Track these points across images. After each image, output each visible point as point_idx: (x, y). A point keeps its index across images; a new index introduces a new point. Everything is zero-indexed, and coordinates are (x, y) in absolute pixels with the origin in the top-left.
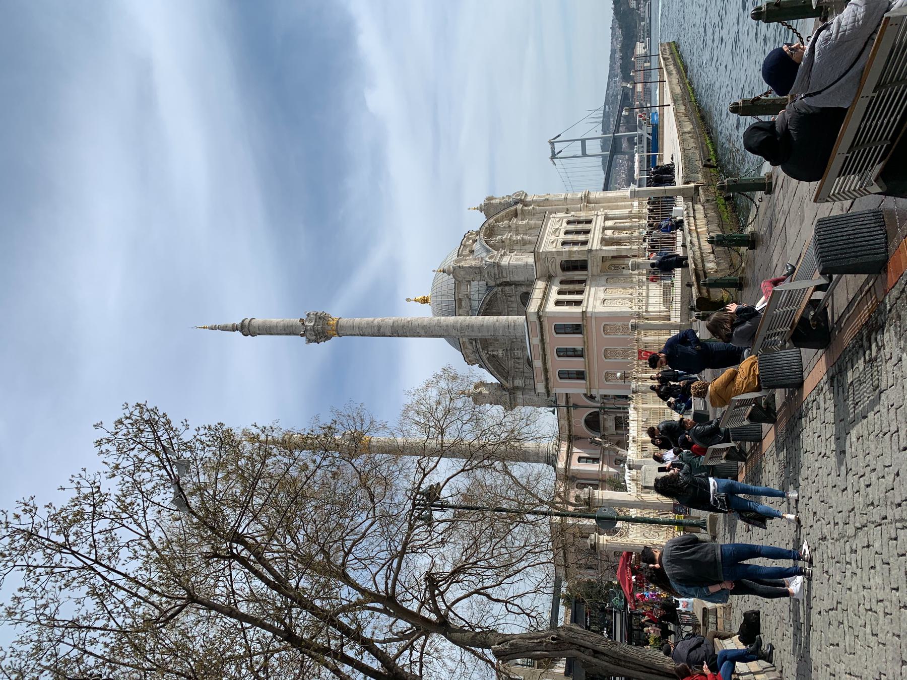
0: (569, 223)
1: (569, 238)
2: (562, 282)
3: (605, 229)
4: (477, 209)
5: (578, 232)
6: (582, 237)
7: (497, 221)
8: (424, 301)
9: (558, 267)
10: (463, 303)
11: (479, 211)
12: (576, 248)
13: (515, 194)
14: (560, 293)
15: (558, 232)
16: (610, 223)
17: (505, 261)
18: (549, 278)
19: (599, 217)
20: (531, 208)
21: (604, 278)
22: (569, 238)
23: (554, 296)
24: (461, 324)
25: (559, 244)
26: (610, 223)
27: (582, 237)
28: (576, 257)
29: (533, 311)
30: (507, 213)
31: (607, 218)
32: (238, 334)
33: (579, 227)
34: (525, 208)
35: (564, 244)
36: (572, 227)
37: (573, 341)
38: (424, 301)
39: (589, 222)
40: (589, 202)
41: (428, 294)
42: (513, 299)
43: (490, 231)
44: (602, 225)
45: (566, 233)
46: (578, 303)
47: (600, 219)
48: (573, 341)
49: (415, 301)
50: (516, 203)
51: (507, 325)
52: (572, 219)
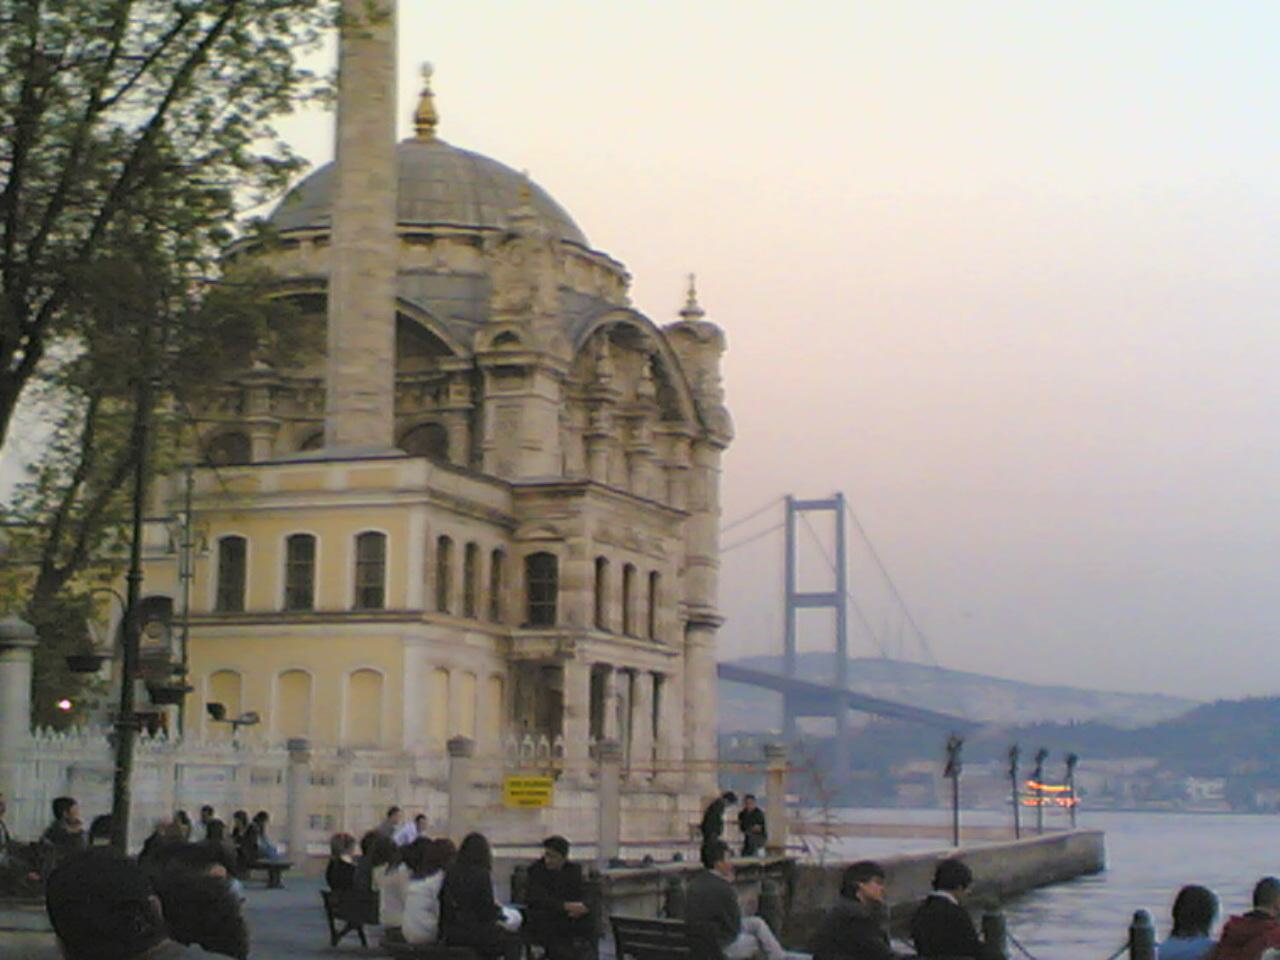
0: (653, 576)
2: (497, 555)
3: (630, 673)
4: (691, 302)
6: (613, 613)
7: (655, 361)
11: (682, 305)
12: (588, 596)
13: (722, 416)
14: (471, 549)
16: (645, 685)
18: (508, 525)
19: (664, 659)
21: (502, 670)
22: (613, 576)
23: (462, 533)
25: (603, 550)
26: (645, 685)
28: (562, 598)
31: (658, 679)
33: (640, 606)
34: (682, 447)
35: (600, 563)
36: (640, 583)
37: (335, 582)
38: (425, 121)
41: (441, 132)
43: (627, 333)
45: (628, 569)
47: (659, 663)
48: (335, 582)
49: (426, 94)
50: (700, 419)
52: (663, 583)
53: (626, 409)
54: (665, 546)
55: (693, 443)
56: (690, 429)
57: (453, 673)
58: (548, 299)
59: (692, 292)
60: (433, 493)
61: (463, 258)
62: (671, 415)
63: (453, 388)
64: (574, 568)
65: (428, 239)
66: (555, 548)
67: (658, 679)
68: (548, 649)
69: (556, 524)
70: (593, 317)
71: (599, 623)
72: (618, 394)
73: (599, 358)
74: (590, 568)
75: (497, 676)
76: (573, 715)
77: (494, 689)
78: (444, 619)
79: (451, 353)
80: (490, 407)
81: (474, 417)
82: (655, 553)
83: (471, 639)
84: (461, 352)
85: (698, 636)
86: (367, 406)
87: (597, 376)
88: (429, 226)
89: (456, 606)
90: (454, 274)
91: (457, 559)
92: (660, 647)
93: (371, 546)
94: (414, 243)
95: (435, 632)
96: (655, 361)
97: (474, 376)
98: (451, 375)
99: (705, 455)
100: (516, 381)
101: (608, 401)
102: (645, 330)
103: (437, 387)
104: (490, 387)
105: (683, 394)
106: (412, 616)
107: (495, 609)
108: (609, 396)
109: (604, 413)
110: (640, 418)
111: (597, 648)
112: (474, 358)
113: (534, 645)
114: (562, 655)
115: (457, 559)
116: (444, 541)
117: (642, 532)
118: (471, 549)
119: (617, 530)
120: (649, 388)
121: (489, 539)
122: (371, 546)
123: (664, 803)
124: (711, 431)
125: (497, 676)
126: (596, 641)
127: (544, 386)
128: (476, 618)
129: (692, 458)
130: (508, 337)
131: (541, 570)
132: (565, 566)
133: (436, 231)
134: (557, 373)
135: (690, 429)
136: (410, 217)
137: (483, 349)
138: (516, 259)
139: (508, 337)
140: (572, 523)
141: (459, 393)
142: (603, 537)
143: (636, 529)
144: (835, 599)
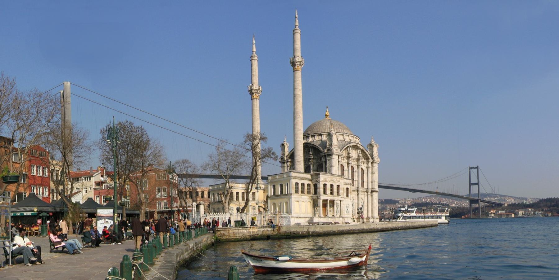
0: (338, 186)
1: (328, 187)
2: (309, 185)
3: (334, 201)
5: (332, 190)
6: (328, 192)
7: (362, 150)
9: (315, 183)
12: (322, 190)
15: (332, 181)
17: (335, 158)
19: (341, 198)
20: (370, 165)
21: (311, 201)
22: (328, 187)
23: (300, 182)
24: (299, 140)
27: (328, 192)
28: (318, 190)
29: (292, 174)
30: (367, 155)
31: (341, 201)
34: (370, 163)
35: (325, 185)
39: (338, 194)
40: (372, 192)
44: (335, 200)
45: (332, 186)
46: (297, 192)
47: (340, 198)
50: (372, 159)
51: (298, 161)
52: (341, 187)
53: (357, 158)
54: (340, 181)
55: (372, 163)
56: (371, 160)
57: (300, 202)
64: (321, 186)
65: (321, 135)
66: (317, 183)
69: (316, 179)
70: (346, 145)
71: (325, 193)
72: (353, 156)
73: (349, 151)
79: (322, 153)
80: (327, 161)
82: (338, 182)
83: (303, 197)
84: (323, 153)
85: (374, 193)
86: (299, 163)
88: (321, 133)
92: (339, 196)
94: (319, 136)
96: (362, 150)
97: (325, 156)
98: (322, 156)
101: (351, 158)
102: (359, 145)
103: (321, 159)
107: (309, 193)
108: (350, 157)
109: (350, 159)
110: (359, 160)
112: (325, 153)
114: (318, 198)
117: (335, 180)
119: (329, 179)
120: (361, 155)
121: (306, 182)
123: (341, 219)
124: (374, 161)
131: (316, 187)
132: (318, 185)
133: (322, 134)
134: (337, 154)
136: (319, 132)
138: (330, 138)
140: (319, 179)
141: (324, 159)
143: (333, 179)
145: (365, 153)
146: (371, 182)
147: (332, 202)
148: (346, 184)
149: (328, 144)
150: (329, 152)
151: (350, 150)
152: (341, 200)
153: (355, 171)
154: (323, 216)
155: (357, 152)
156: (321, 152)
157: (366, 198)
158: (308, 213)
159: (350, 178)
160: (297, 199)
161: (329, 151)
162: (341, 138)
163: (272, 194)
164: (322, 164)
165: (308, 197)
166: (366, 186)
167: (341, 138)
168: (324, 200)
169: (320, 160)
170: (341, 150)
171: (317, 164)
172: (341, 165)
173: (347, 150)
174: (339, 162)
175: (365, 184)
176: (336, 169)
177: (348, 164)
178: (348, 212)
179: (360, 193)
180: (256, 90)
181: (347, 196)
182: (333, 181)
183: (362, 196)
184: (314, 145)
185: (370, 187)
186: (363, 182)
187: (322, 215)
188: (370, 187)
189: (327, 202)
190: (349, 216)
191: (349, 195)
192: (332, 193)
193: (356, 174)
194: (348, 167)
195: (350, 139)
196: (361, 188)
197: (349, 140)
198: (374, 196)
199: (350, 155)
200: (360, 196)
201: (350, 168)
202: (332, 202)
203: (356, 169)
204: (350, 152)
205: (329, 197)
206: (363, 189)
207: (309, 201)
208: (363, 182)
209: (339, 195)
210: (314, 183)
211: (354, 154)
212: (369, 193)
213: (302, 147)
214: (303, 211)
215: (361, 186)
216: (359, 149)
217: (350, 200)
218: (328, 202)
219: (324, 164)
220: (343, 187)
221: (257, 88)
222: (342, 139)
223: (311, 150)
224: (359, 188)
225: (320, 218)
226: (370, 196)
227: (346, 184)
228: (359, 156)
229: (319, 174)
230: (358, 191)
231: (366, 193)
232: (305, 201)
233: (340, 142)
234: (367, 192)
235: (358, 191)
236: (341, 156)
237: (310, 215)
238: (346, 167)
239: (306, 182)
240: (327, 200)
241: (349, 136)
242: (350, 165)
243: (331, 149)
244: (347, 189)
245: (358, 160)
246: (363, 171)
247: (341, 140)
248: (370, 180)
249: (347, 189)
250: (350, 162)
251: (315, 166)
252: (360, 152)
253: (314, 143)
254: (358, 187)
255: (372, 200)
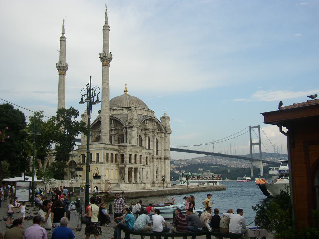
0: (141, 156)
1: (133, 156)
2: (116, 155)
5: (135, 159)
6: (133, 161)
8: (126, 92)
9: (122, 153)
10: (121, 111)
11: (164, 114)
12: (128, 159)
13: (170, 129)
14: (112, 154)
18: (118, 151)
19: (143, 166)
21: (118, 169)
22: (133, 156)
23: (110, 152)
24: (106, 115)
25: (130, 153)
27: (133, 161)
28: (125, 160)
31: (142, 169)
32: (104, 24)
33: (138, 159)
34: (163, 134)
35: (130, 155)
36: (138, 157)
38: (126, 92)
39: (141, 163)
40: (165, 159)
41: (128, 93)
42: (122, 131)
43: (152, 120)
45: (136, 155)
47: (142, 167)
50: (165, 130)
52: (143, 156)
54: (142, 151)
56: (164, 131)
58: (135, 116)
59: (165, 112)
60: (104, 148)
61: (125, 112)
62: (161, 130)
63: (124, 130)
64: (127, 156)
65: (122, 109)
66: (124, 153)
67: (142, 169)
68: (123, 166)
69: (124, 150)
70: (144, 119)
71: (130, 162)
74: (128, 156)
75: (117, 169)
76: (126, 174)
77: (117, 171)
78: (108, 163)
80: (128, 132)
81: (126, 133)
83: (112, 165)
84: (125, 125)
85: (166, 161)
87: (146, 126)
89: (109, 161)
90: (125, 114)
91: (110, 156)
93: (98, 154)
95: (106, 165)
96: (157, 123)
97: (126, 128)
98: (124, 128)
99: (167, 135)
100: (131, 129)
102: (154, 119)
103: (122, 129)
104: (128, 130)
105: (162, 127)
106: (102, 163)
107: (116, 161)
111: (130, 165)
112: (126, 126)
113: (122, 166)
115: (110, 156)
116: (107, 154)
117: (138, 150)
118: (112, 154)
119: (133, 150)
120: (156, 127)
122: (98, 154)
123: (143, 184)
125: (117, 169)
126: (129, 165)
127: (135, 129)
128: (113, 162)
129: (165, 136)
130: (130, 123)
131: (122, 156)
132: (125, 155)
134: (137, 127)
135: (164, 131)
137: (127, 125)
139: (130, 123)
142: (131, 151)
144: (259, 144)
145: (159, 125)
146: (164, 151)
147: (136, 169)
148: (146, 153)
149: (129, 118)
150: (130, 125)
151: (147, 123)
152: (143, 167)
153: (150, 141)
154: (129, 182)
155: (153, 124)
156: (122, 125)
157: (159, 164)
158: (115, 180)
159: (147, 148)
160: (107, 167)
161: (130, 124)
162: (139, 112)
163: (81, 162)
164: (123, 135)
165: (116, 166)
166: (159, 154)
167: (139, 112)
168: (129, 168)
169: (121, 131)
170: (140, 123)
171: (118, 134)
172: (140, 136)
173: (145, 123)
174: (138, 133)
175: (159, 152)
176: (135, 141)
177: (145, 135)
178: (147, 178)
179: (155, 160)
180: (64, 67)
181: (147, 164)
182: (136, 151)
183: (157, 163)
184: (116, 118)
185: (163, 155)
186: (157, 151)
187: (128, 181)
188: (163, 155)
189: (132, 170)
190: (149, 182)
191: (149, 163)
192: (135, 162)
193: (151, 143)
194: (145, 137)
195: (147, 113)
196: (156, 156)
197: (146, 114)
198: (166, 163)
199: (147, 127)
200: (155, 163)
201: (147, 138)
202: (136, 169)
203: (151, 139)
204: (147, 125)
205: (134, 166)
206: (157, 157)
207: (116, 169)
208: (157, 151)
209: (141, 164)
210: (121, 153)
211: (150, 126)
212: (163, 161)
213: (108, 121)
214: (112, 178)
215: (155, 154)
216: (154, 122)
217: (149, 167)
218: (133, 169)
219: (125, 135)
220: (144, 156)
221: (65, 66)
222: (140, 113)
223: (113, 123)
224: (154, 156)
225: (126, 184)
226: (163, 163)
227: (146, 153)
228: (154, 128)
229: (126, 146)
230: (153, 159)
231: (159, 160)
232: (113, 168)
233: (139, 116)
234: (161, 159)
235: (153, 159)
236: (140, 128)
237: (117, 181)
238: (143, 138)
239: (115, 153)
240: (132, 168)
241: (146, 110)
242: (147, 136)
243: (132, 123)
244: (147, 157)
245: (153, 131)
246: (157, 141)
247: (139, 114)
248: (163, 149)
249: (147, 157)
250: (147, 133)
251: (116, 136)
252: (155, 124)
253: (116, 116)
254: (153, 155)
255: (164, 167)
